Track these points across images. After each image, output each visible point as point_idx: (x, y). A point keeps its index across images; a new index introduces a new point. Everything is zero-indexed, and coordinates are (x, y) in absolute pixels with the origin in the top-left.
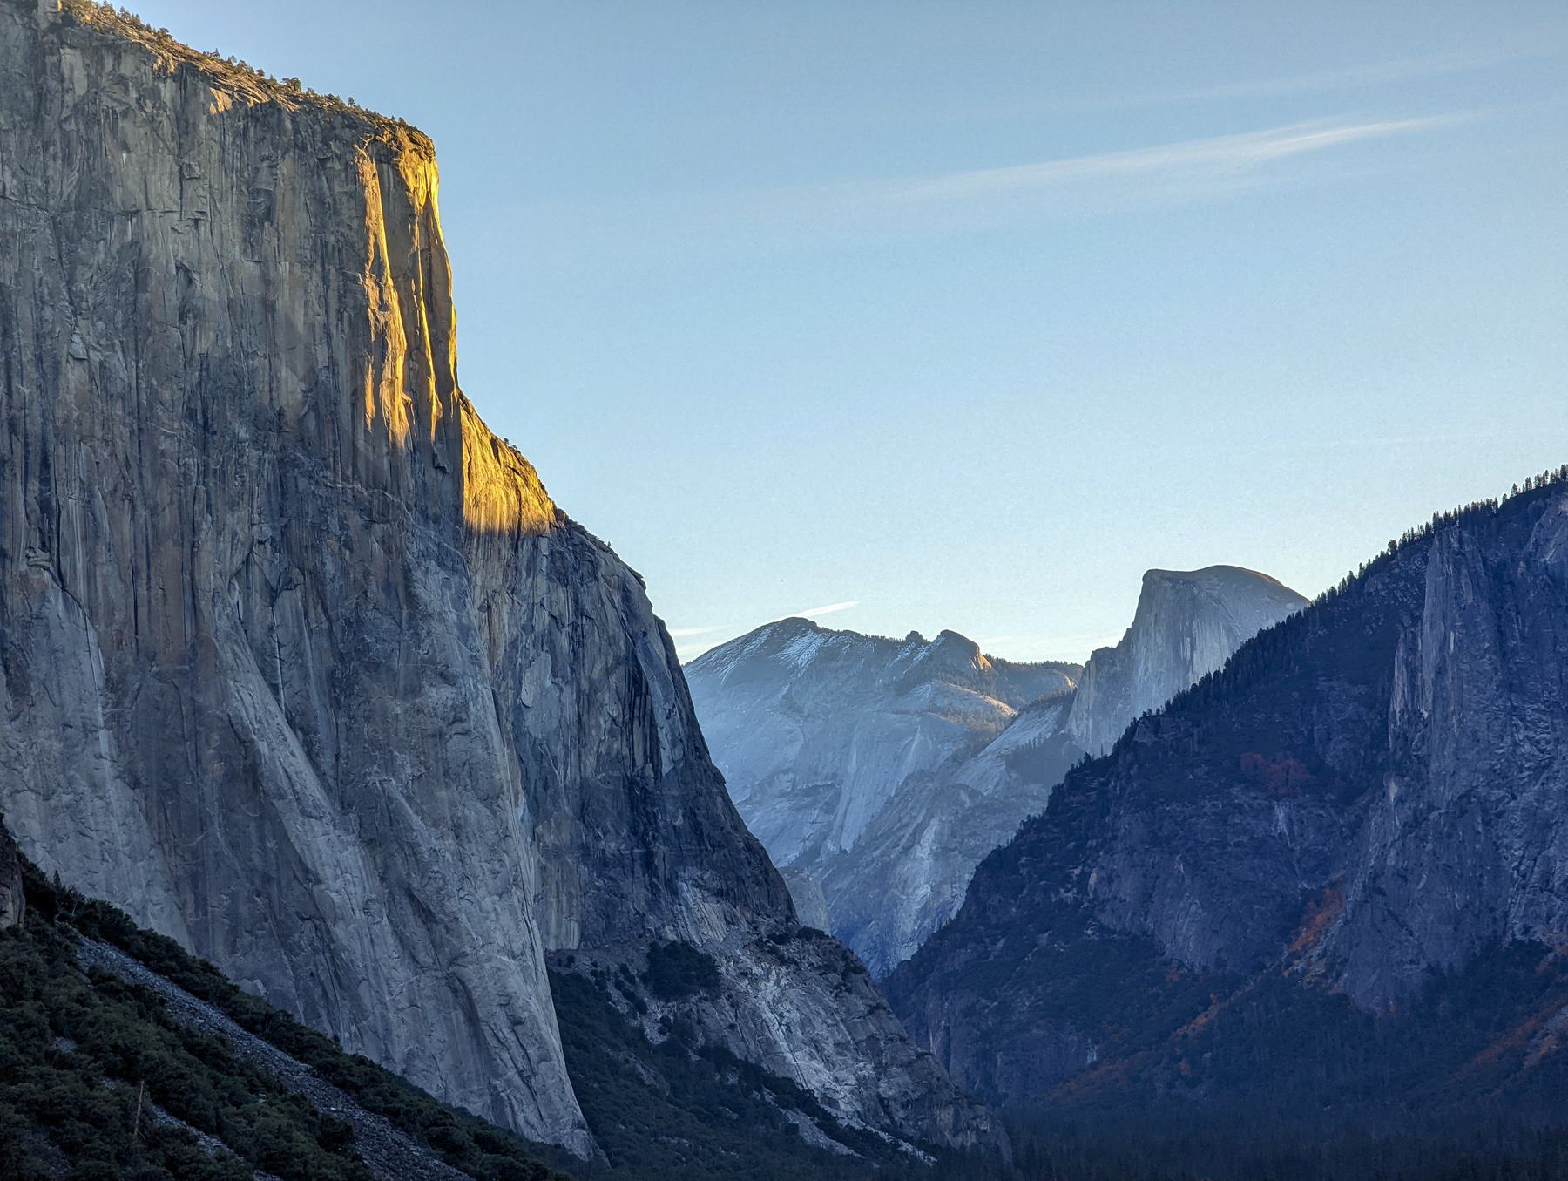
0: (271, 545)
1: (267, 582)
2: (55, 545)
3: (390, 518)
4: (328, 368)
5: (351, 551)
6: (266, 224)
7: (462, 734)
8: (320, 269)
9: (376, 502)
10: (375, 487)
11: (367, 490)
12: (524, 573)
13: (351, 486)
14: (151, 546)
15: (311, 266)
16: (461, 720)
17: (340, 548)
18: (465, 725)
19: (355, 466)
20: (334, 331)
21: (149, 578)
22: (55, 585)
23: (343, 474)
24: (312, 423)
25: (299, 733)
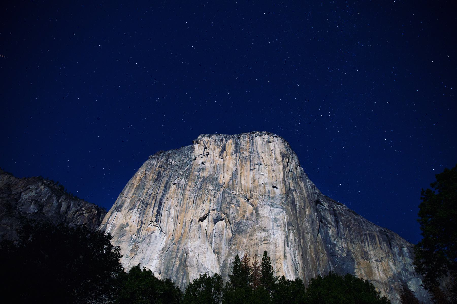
0: (217, 210)
1: (213, 218)
2: (160, 221)
3: (253, 198)
4: (235, 171)
5: (240, 207)
6: (224, 151)
7: (266, 243)
8: (235, 154)
9: (248, 195)
10: (247, 191)
11: (245, 192)
12: (398, 256)
13: (241, 193)
14: (179, 214)
15: (234, 154)
16: (267, 240)
17: (236, 207)
18: (268, 241)
19: (241, 188)
20: (237, 164)
21: (177, 221)
22: (159, 230)
23: (239, 190)
24: (231, 182)
25: (216, 254)
